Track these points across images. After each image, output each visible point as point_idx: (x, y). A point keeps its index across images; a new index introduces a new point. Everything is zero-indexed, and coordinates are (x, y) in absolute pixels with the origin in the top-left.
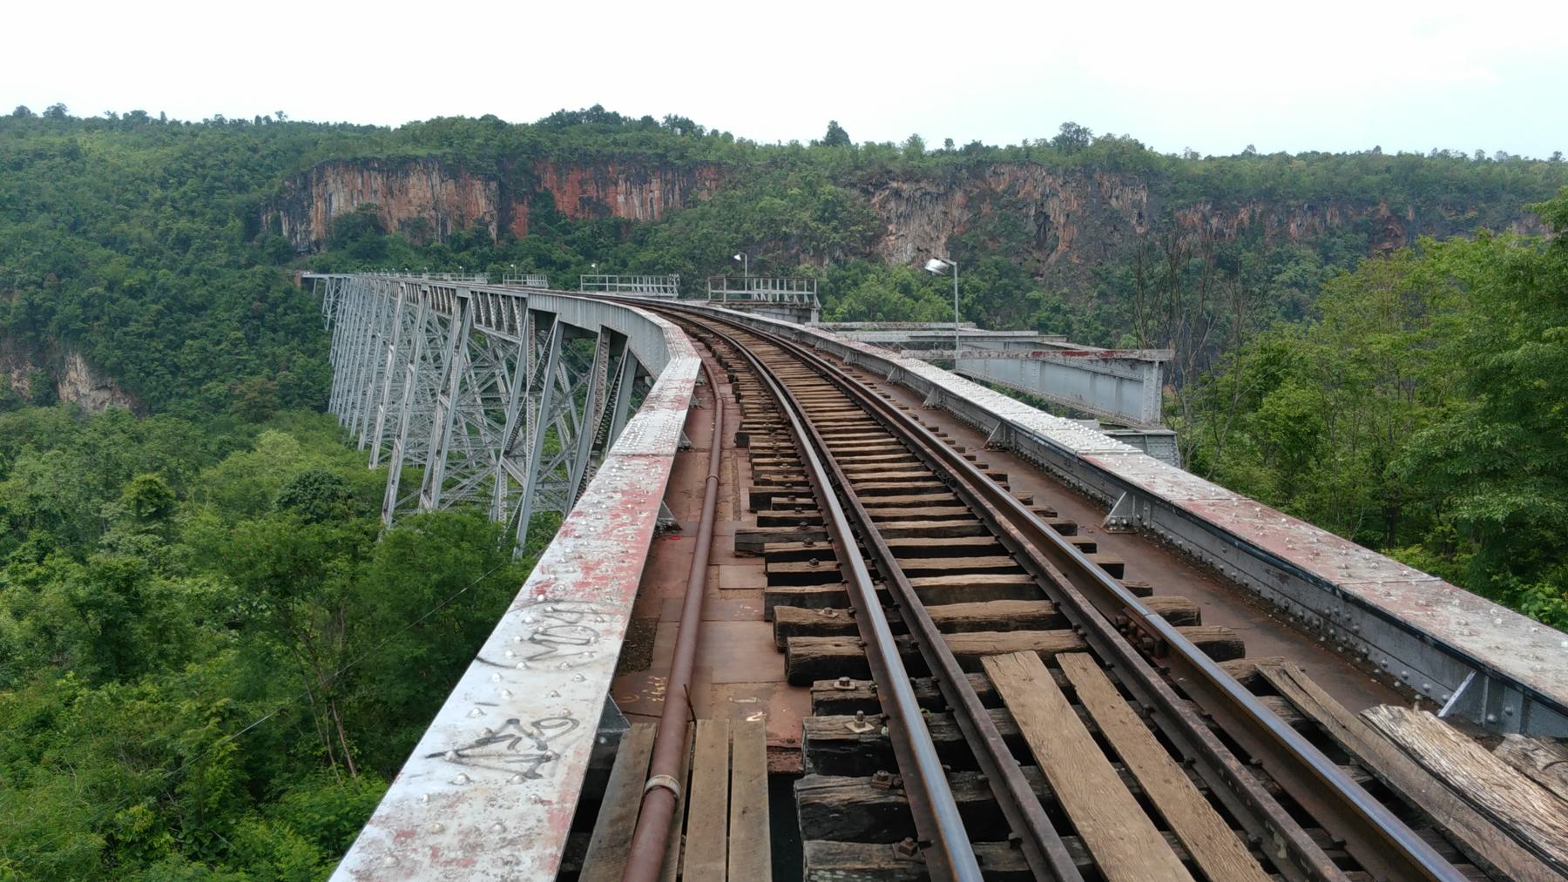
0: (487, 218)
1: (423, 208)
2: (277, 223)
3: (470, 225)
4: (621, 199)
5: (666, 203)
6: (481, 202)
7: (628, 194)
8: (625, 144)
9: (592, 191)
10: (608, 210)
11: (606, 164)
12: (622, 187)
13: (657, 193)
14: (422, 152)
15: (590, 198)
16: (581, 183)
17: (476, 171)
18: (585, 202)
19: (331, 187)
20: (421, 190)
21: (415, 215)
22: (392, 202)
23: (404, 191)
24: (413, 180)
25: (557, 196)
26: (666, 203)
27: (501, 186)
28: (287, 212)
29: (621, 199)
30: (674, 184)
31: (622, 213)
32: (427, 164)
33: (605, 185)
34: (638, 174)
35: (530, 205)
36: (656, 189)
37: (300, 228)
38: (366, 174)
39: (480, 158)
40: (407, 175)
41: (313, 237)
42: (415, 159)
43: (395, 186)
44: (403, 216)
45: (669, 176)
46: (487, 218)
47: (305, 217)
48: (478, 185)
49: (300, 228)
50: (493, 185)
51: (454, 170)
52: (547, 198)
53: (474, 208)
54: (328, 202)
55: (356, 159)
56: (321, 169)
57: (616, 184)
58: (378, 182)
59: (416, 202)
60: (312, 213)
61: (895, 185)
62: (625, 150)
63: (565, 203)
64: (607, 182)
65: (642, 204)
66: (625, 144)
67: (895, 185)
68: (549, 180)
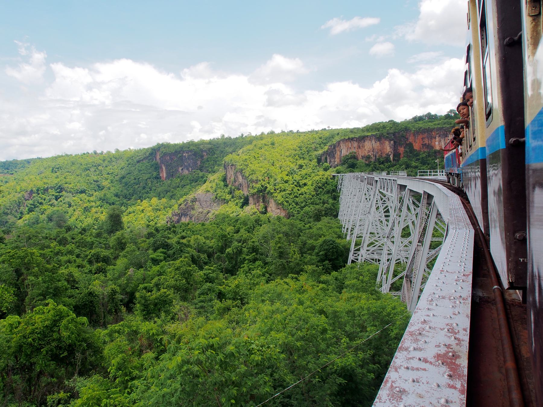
1: (369, 151)
3: (384, 155)
4: (437, 143)
6: (388, 148)
7: (440, 141)
8: (438, 124)
9: (426, 141)
10: (432, 147)
11: (431, 131)
12: (437, 139)
14: (369, 134)
16: (422, 139)
19: (342, 147)
20: (368, 145)
21: (367, 154)
23: (363, 146)
24: (366, 143)
27: (395, 142)
29: (437, 143)
32: (370, 138)
33: (431, 139)
34: (444, 134)
35: (404, 148)
37: (332, 160)
39: (388, 134)
40: (365, 141)
41: (336, 163)
42: (367, 136)
43: (361, 145)
44: (363, 155)
47: (334, 157)
48: (387, 142)
50: (392, 142)
51: (379, 138)
52: (410, 145)
55: (349, 138)
56: (339, 143)
57: (435, 138)
58: (355, 144)
59: (367, 150)
60: (336, 156)
62: (439, 126)
63: (417, 146)
64: (432, 138)
66: (438, 124)
68: (411, 139)
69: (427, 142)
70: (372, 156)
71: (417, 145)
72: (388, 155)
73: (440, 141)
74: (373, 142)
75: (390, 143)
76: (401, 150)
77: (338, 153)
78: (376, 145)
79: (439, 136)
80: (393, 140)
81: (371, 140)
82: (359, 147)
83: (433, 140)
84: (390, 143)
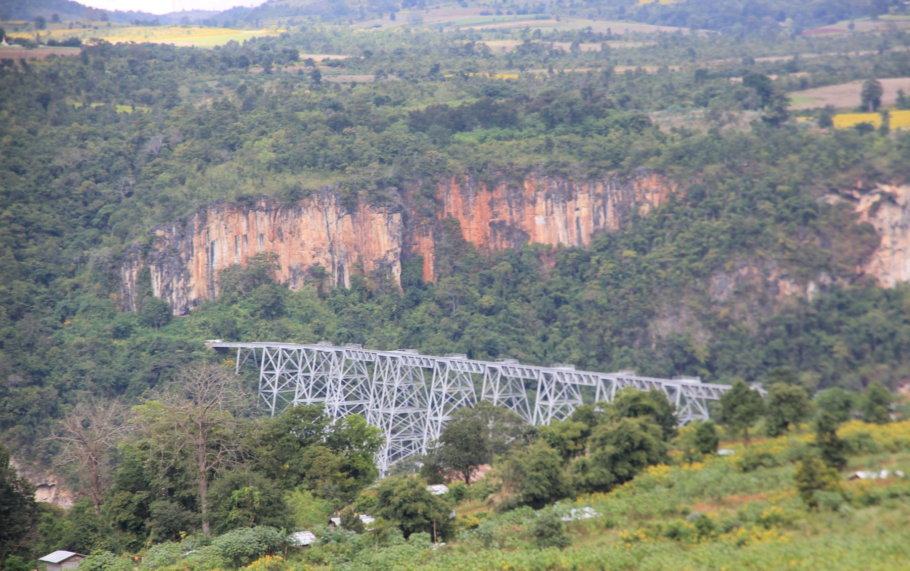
0: (391, 258)
1: (317, 251)
2: (145, 277)
4: (540, 220)
5: (596, 222)
7: (549, 214)
9: (505, 214)
10: (525, 235)
11: (521, 180)
12: (541, 205)
13: (584, 212)
15: (502, 223)
16: (491, 204)
17: (378, 201)
18: (497, 227)
21: (310, 262)
22: (282, 246)
23: (295, 232)
25: (464, 222)
26: (596, 222)
27: (405, 218)
28: (160, 266)
29: (540, 220)
30: (605, 199)
31: (542, 237)
33: (521, 204)
35: (436, 238)
36: (583, 204)
37: (177, 284)
38: (251, 215)
40: (299, 212)
41: (193, 296)
43: (285, 228)
44: (295, 263)
45: (600, 189)
46: (391, 258)
48: (379, 219)
49: (177, 284)
50: (397, 217)
52: (452, 227)
53: (373, 247)
54: (210, 251)
57: (534, 202)
58: (263, 223)
59: (310, 244)
61: (887, 189)
63: (473, 231)
65: (567, 225)
67: (887, 189)
69: (507, 217)
70: (329, 270)
71: (473, 225)
72: (384, 266)
73: (549, 214)
74: (332, 216)
75: (390, 218)
76: (425, 245)
77: (201, 255)
78: (341, 227)
79: (548, 197)
80: (399, 209)
81: (321, 208)
82: (278, 234)
83: (528, 208)
84: (390, 218)
